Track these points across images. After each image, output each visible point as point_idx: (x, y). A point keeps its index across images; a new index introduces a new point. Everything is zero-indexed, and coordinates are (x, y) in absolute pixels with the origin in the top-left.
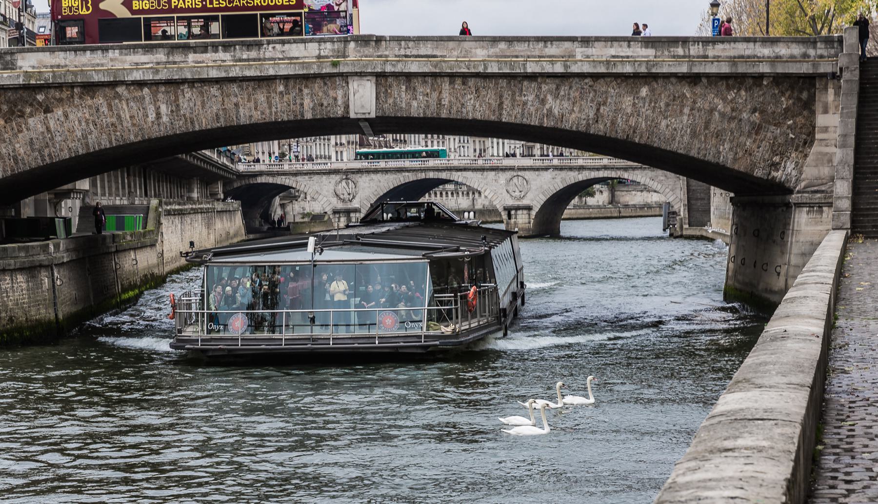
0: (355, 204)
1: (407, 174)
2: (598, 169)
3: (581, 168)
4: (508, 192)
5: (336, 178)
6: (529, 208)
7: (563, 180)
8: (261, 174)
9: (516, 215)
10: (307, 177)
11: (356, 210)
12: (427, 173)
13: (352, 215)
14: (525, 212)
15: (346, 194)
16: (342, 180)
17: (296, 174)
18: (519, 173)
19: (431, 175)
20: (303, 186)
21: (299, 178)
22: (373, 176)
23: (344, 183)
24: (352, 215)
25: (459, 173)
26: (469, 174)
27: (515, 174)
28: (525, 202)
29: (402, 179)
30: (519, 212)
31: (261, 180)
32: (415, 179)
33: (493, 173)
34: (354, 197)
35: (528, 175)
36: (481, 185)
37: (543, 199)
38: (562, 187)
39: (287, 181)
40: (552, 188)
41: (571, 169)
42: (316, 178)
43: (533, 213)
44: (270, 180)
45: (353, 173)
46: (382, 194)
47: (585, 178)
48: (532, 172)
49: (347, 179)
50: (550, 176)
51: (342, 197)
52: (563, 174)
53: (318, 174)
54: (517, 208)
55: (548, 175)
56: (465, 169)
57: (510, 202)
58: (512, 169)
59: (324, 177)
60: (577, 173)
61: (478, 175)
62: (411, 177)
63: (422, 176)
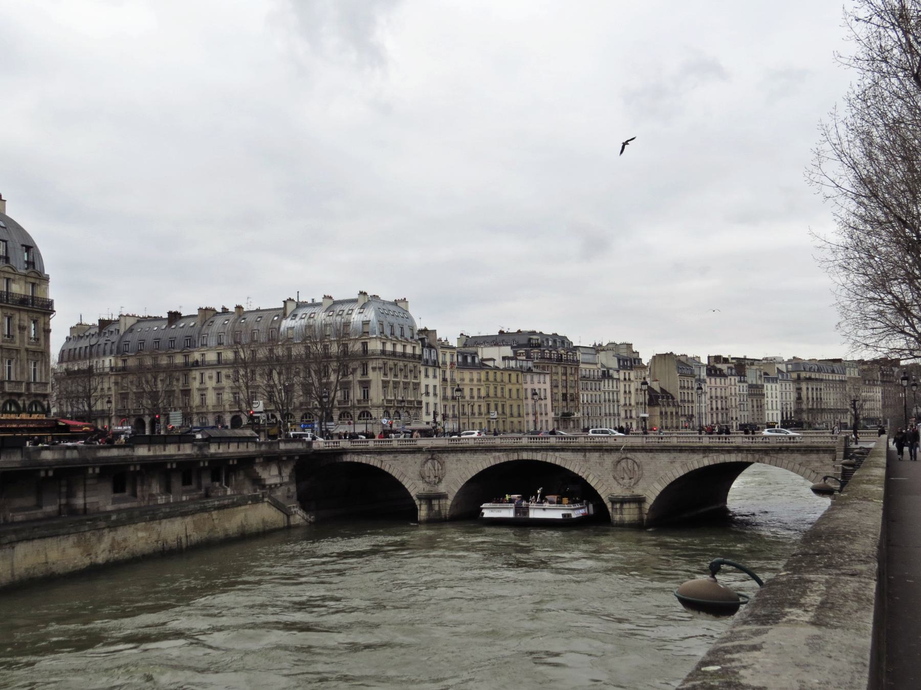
0: (442, 488)
1: (497, 454)
2: (729, 451)
3: (706, 450)
4: (615, 478)
5: (420, 458)
6: (639, 500)
7: (684, 464)
8: (344, 452)
9: (621, 508)
10: (391, 456)
11: (442, 496)
12: (520, 454)
13: (435, 502)
14: (633, 506)
15: (432, 477)
16: (427, 460)
17: (380, 452)
18: (629, 455)
19: (525, 456)
20: (388, 466)
21: (384, 457)
22: (461, 456)
23: (429, 464)
24: (435, 502)
25: (557, 454)
26: (568, 455)
27: (623, 456)
28: (638, 491)
29: (492, 460)
30: (626, 506)
31: (348, 458)
32: (506, 460)
33: (597, 454)
34: (440, 481)
35: (639, 457)
36: (583, 470)
37: (658, 488)
38: (682, 473)
39: (372, 460)
40: (670, 475)
41: (693, 450)
42: (401, 457)
43: (647, 506)
44: (356, 459)
45: (439, 452)
46: (470, 477)
47: (712, 463)
48: (644, 454)
49: (433, 459)
50: (667, 459)
51: (427, 479)
52: (683, 456)
53: (403, 452)
54: (623, 501)
55: (664, 458)
56: (563, 449)
57: (619, 491)
58: (616, 449)
59: (409, 457)
60: (701, 456)
61: (580, 456)
62: (503, 458)
63: (514, 457)
